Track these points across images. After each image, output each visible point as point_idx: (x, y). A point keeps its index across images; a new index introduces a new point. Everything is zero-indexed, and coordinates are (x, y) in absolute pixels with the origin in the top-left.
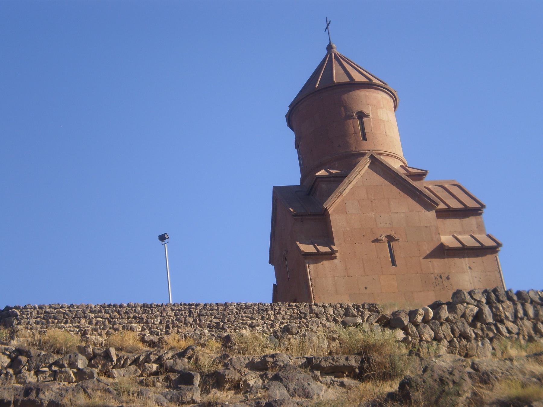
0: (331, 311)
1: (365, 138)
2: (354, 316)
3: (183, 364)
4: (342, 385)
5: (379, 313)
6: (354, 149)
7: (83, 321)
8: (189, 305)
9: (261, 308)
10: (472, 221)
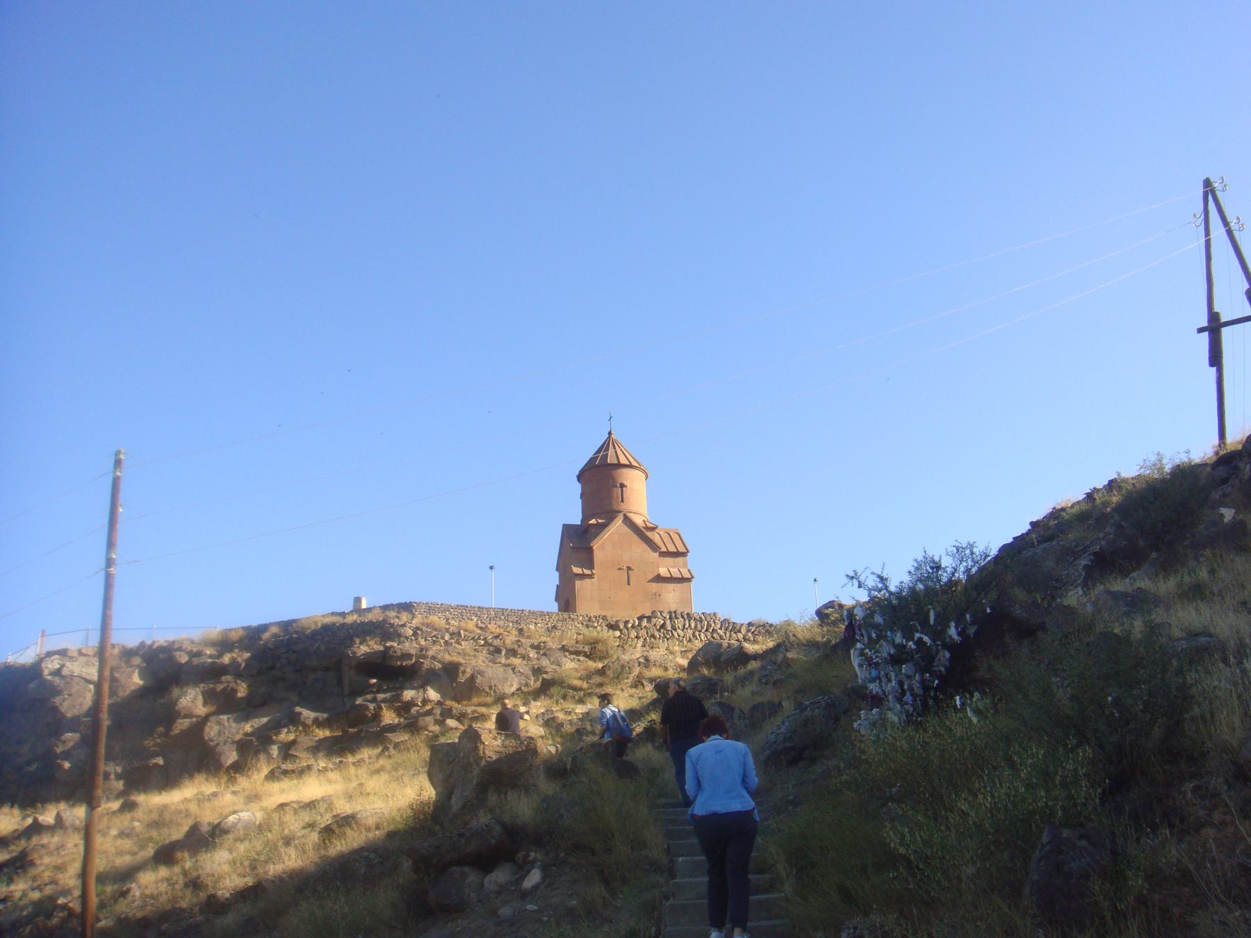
0: (581, 618)
1: (622, 501)
2: (593, 622)
3: (497, 642)
4: (579, 660)
5: (607, 621)
6: (614, 507)
7: (447, 613)
8: (503, 609)
9: (542, 614)
10: (681, 559)
